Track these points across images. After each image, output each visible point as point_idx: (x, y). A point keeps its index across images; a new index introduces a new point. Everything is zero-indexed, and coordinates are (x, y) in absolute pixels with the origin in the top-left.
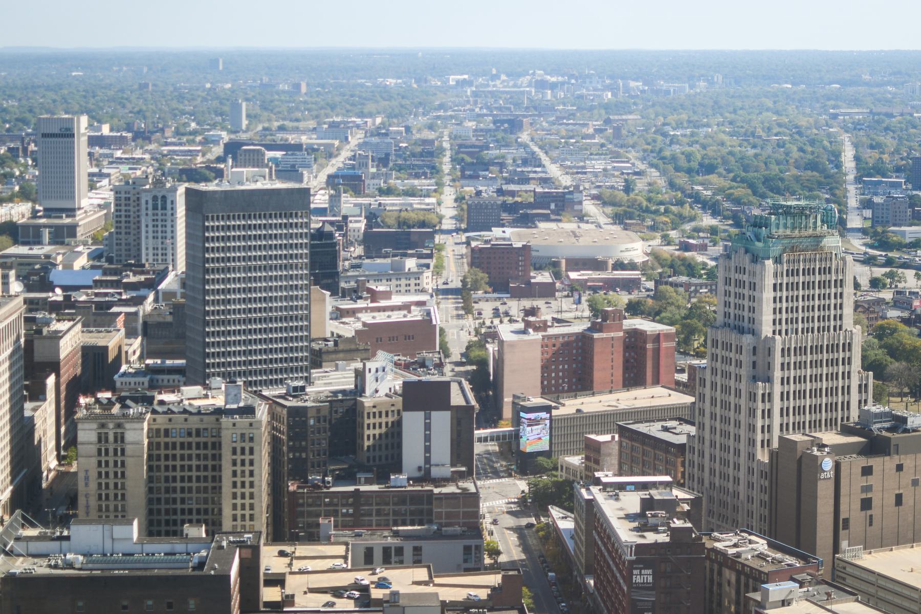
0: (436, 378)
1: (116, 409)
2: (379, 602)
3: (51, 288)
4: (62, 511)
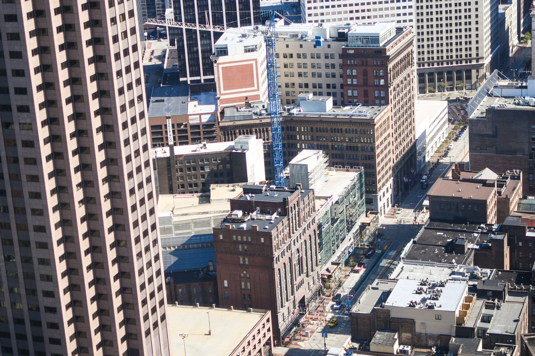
4: (521, 71)
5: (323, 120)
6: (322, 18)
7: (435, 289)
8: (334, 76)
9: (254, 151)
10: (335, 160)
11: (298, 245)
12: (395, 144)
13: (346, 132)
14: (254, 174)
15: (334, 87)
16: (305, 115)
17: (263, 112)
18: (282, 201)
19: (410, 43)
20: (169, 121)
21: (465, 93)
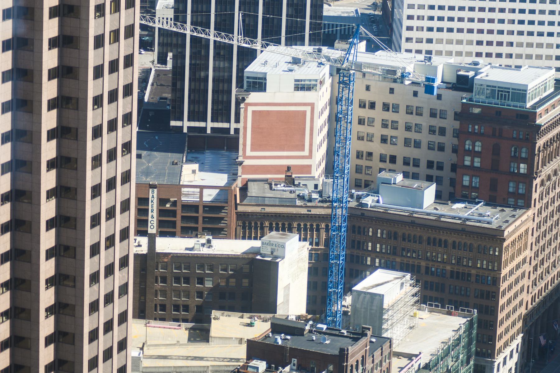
5: (417, 221)
6: (429, 47)
8: (441, 148)
10: (429, 293)
12: (533, 277)
13: (454, 247)
14: (288, 301)
15: (440, 167)
16: (386, 209)
17: (315, 196)
18: (337, 352)
20: (153, 192)
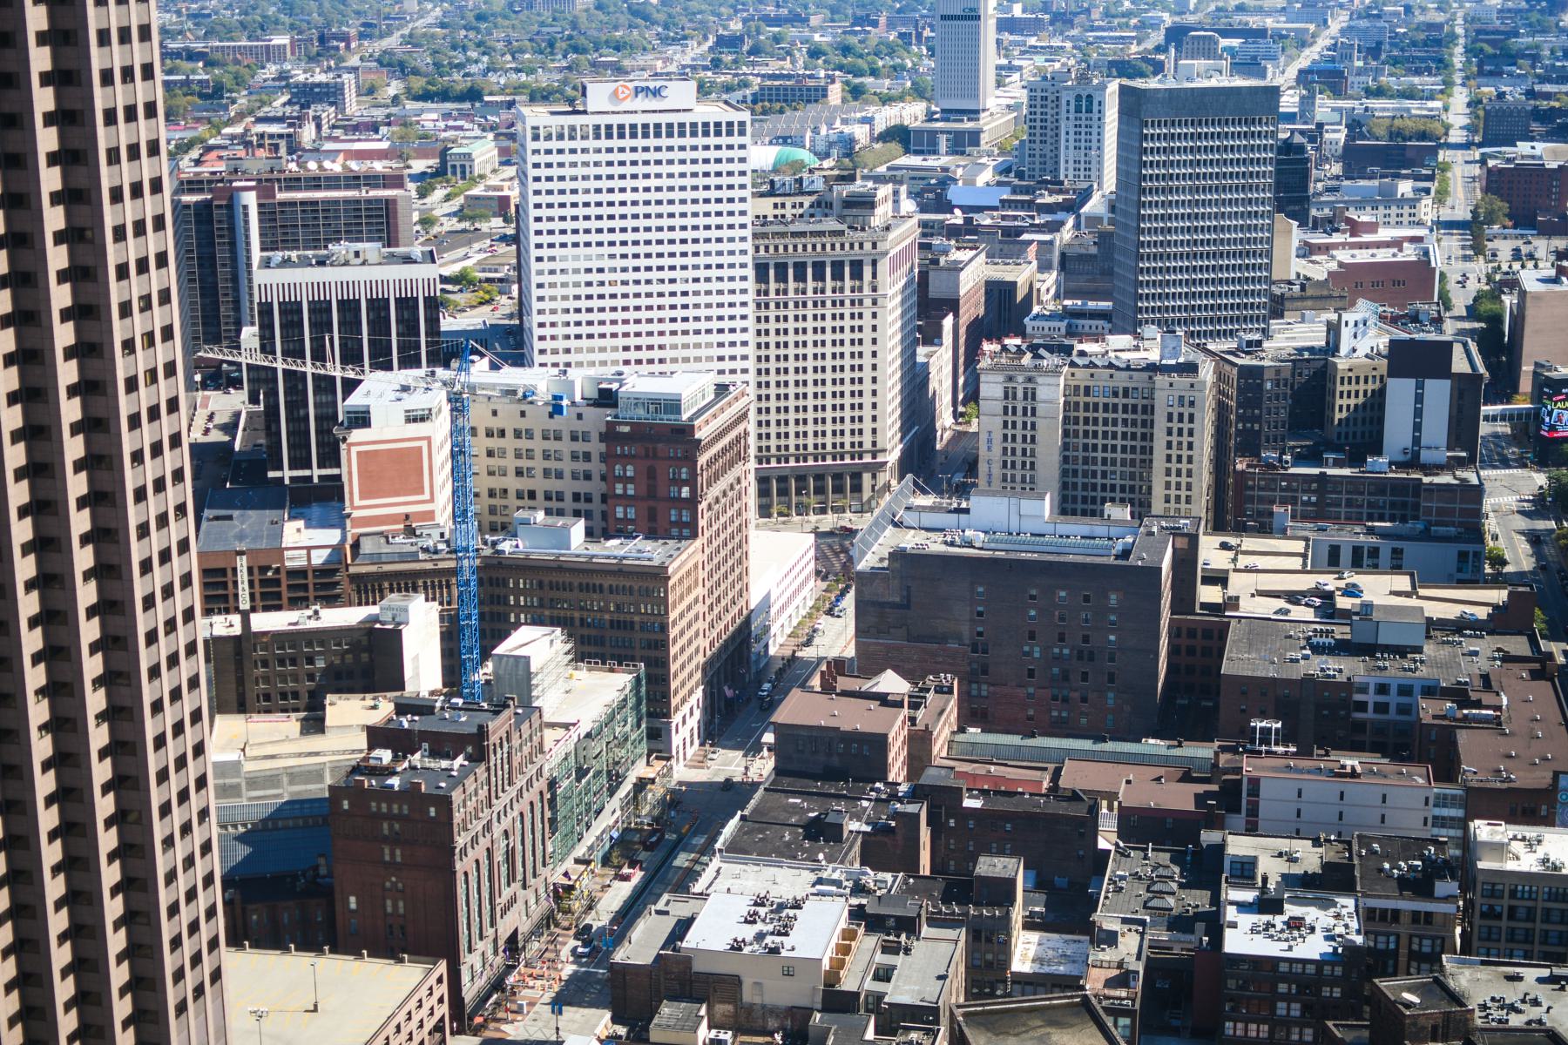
0: (1433, 337)
1: (1027, 359)
2: (1346, 614)
3: (949, 208)
4: (958, 478)
7: (783, 914)
8: (588, 477)
9: (421, 630)
10: (587, 649)
11: (506, 823)
17: (441, 546)
19: (743, 416)
21: (848, 519)
